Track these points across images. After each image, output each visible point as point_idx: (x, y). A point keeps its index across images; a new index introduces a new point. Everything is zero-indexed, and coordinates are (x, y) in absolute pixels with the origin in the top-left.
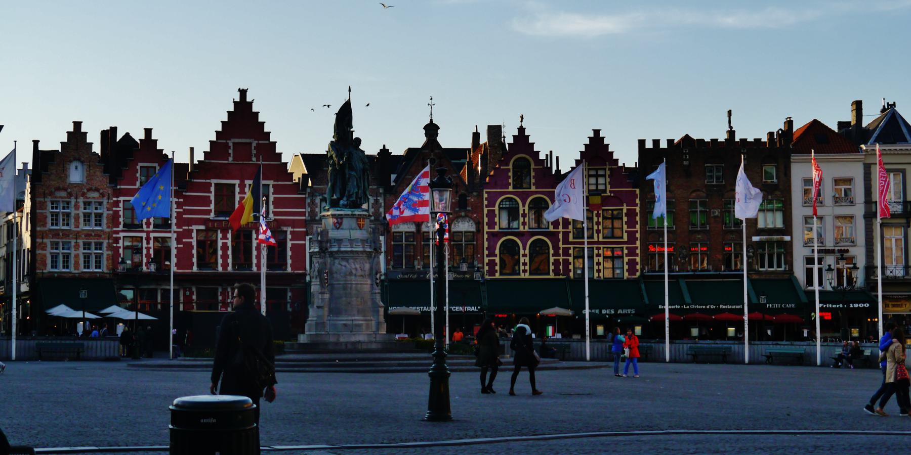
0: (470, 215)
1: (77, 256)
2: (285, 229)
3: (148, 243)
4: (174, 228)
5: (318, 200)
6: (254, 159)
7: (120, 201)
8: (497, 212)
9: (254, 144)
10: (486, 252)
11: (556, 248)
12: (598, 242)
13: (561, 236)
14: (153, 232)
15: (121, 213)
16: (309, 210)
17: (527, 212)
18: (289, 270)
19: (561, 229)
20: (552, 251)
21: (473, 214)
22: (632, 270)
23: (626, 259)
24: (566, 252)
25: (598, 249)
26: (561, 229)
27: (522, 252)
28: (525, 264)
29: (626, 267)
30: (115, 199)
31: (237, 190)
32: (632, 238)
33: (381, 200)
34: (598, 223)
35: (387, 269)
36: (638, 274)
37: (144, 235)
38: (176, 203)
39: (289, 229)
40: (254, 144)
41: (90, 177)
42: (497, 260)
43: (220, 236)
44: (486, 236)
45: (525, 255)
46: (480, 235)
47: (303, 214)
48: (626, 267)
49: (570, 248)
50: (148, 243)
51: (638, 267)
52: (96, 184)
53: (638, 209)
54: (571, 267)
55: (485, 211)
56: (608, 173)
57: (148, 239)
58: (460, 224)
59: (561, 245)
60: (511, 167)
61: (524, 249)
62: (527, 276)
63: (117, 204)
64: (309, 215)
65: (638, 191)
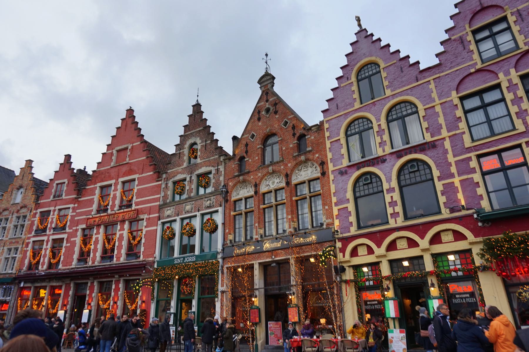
0: (310, 156)
2: (141, 217)
3: (47, 245)
4: (67, 230)
5: (170, 184)
6: (127, 159)
7: (36, 213)
8: (343, 141)
9: (130, 148)
13: (447, 144)
14: (53, 234)
15: (36, 222)
16: (163, 194)
17: (384, 126)
19: (445, 133)
21: (314, 154)
26: (445, 133)
27: (386, 186)
28: (393, 204)
30: (35, 212)
33: (222, 168)
35: (223, 245)
37: (45, 238)
38: (74, 208)
39: (145, 216)
40: (130, 148)
41: (24, 198)
42: (351, 207)
43: (95, 231)
44: (332, 177)
45: (391, 190)
46: (326, 178)
47: (157, 200)
49: (470, 159)
50: (47, 245)
52: (26, 202)
54: (481, 191)
58: (303, 173)
59: (451, 159)
60: (353, 79)
61: (389, 180)
63: (34, 216)
64: (163, 200)
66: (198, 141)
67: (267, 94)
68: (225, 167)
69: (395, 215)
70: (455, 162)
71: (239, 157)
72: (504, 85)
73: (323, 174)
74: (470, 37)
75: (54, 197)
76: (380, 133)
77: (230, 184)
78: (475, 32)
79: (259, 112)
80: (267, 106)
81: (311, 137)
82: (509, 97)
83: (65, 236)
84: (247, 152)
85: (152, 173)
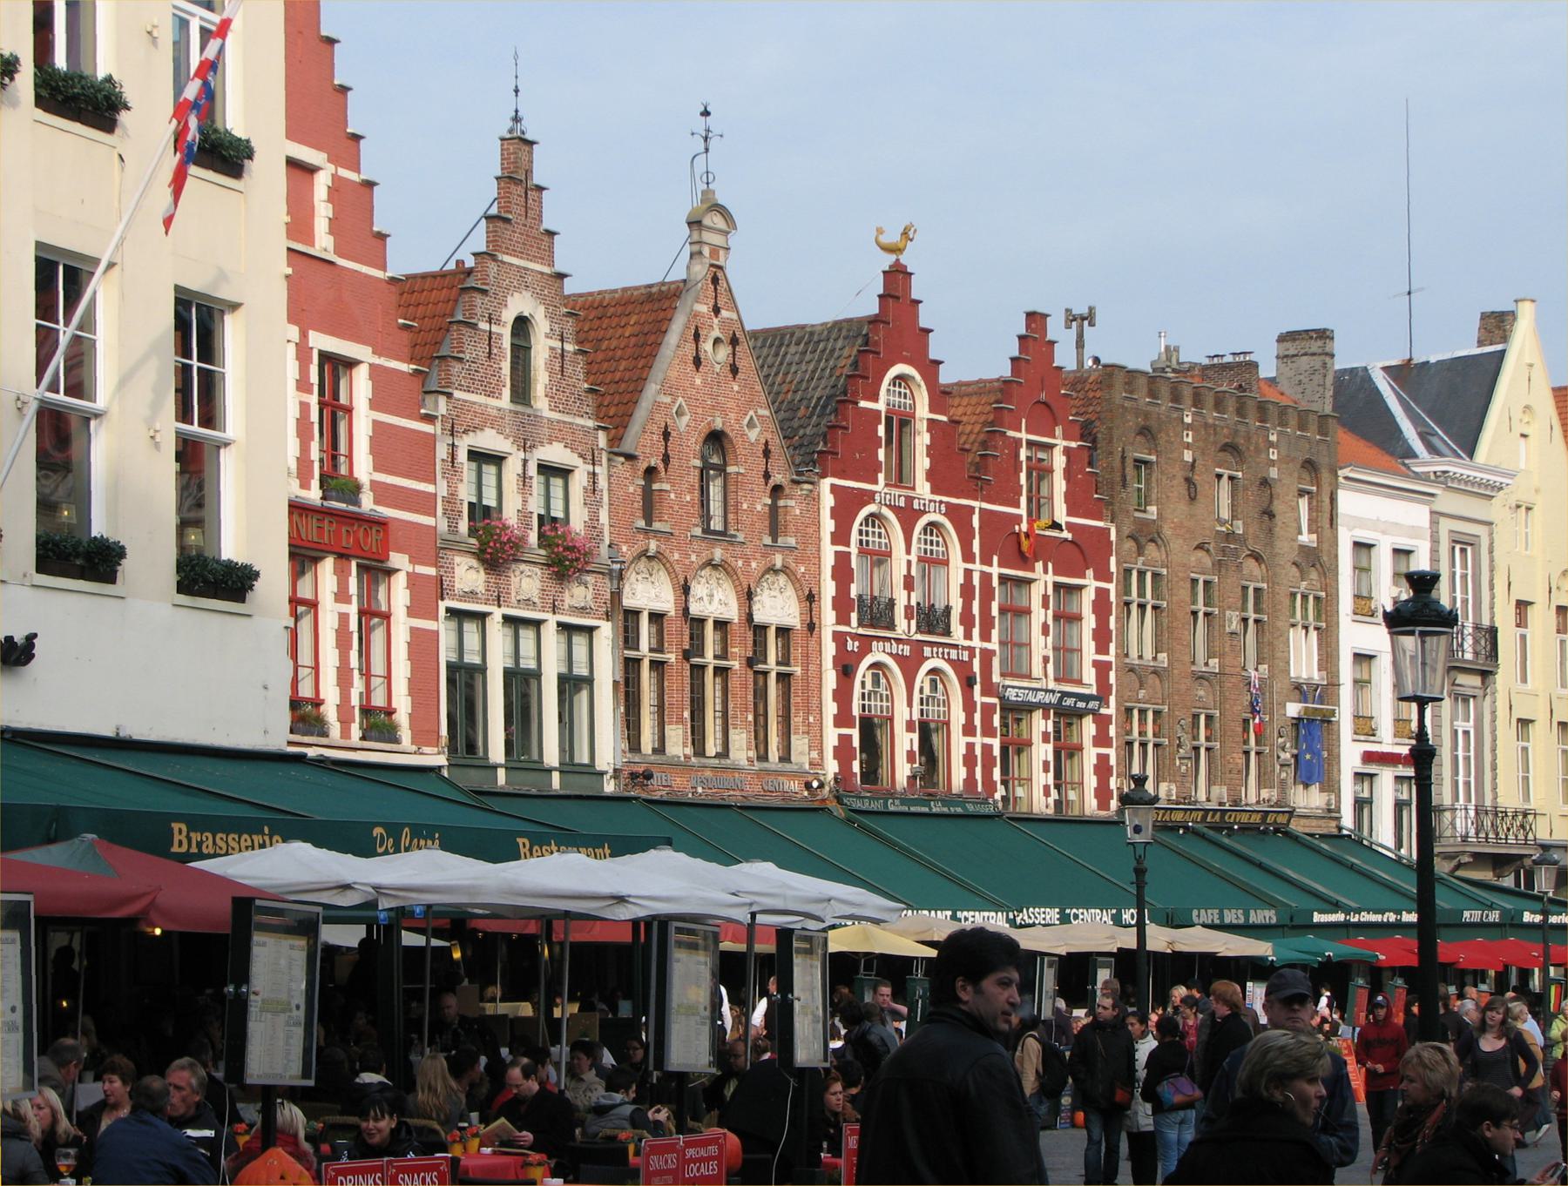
11: (969, 706)
16: (441, 489)
19: (976, 642)
20: (958, 717)
23: (1090, 755)
27: (902, 713)
29: (1091, 782)
46: (813, 643)
53: (1112, 587)
55: (828, 560)
56: (1059, 461)
60: (881, 406)
61: (910, 704)
65: (1113, 537)
67: (715, 280)
68: (610, 476)
70: (983, 704)
71: (645, 465)
77: (624, 548)
78: (1030, 444)
79: (697, 337)
80: (716, 333)
81: (793, 505)
84: (666, 459)
85: (405, 367)
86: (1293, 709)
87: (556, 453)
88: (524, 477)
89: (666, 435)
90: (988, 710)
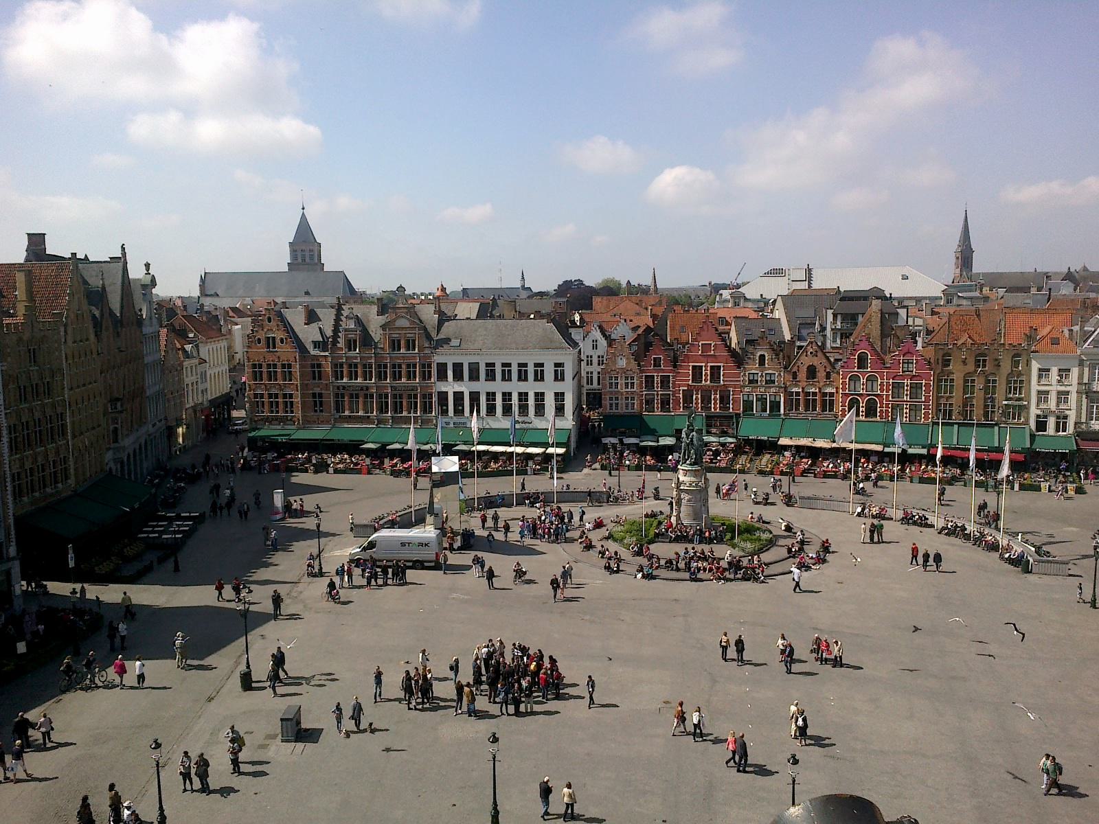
1: (622, 404)
4: (671, 389)
8: (847, 382)
10: (840, 404)
11: (882, 403)
12: (907, 401)
16: (742, 379)
18: (731, 410)
19: (885, 393)
22: (926, 418)
23: (923, 411)
24: (887, 406)
25: (907, 405)
26: (885, 393)
27: (861, 405)
28: (862, 412)
31: (704, 368)
32: (927, 400)
33: (782, 374)
34: (907, 390)
36: (930, 420)
37: (656, 393)
45: (863, 407)
48: (923, 416)
51: (930, 416)
56: (915, 361)
57: (658, 395)
60: (856, 357)
61: (863, 403)
62: (864, 418)
66: (766, 355)
69: (862, 415)
72: (906, 384)
73: (837, 392)
74: (901, 361)
75: (654, 367)
76: (863, 384)
79: (807, 352)
80: (811, 351)
82: (906, 388)
83: (671, 393)
84: (798, 370)
86: (1006, 402)
87: (770, 372)
88: (762, 376)
89: (798, 366)
90: (887, 406)
